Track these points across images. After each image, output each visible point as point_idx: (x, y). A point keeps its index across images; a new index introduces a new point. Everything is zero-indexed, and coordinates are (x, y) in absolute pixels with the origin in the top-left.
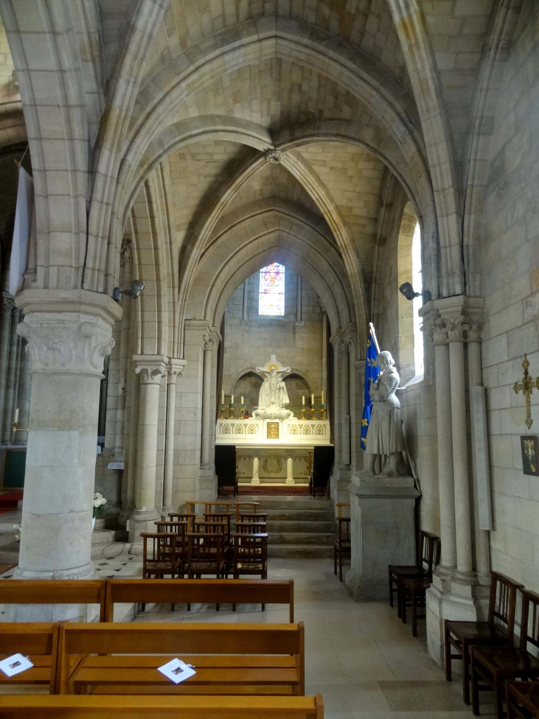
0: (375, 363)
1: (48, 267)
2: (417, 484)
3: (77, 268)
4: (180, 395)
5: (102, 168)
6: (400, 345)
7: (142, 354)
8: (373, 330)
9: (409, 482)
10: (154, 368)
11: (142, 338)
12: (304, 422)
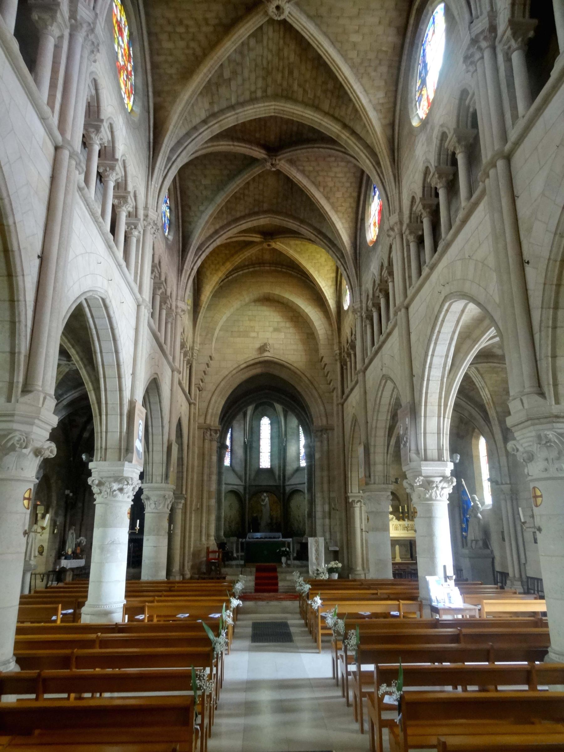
0: (466, 499)
1: (375, 476)
2: (492, 552)
3: (384, 476)
5: (391, 444)
6: (477, 490)
7: (351, 492)
8: (464, 483)
9: (488, 551)
10: (358, 499)
11: (351, 484)
12: (401, 522)
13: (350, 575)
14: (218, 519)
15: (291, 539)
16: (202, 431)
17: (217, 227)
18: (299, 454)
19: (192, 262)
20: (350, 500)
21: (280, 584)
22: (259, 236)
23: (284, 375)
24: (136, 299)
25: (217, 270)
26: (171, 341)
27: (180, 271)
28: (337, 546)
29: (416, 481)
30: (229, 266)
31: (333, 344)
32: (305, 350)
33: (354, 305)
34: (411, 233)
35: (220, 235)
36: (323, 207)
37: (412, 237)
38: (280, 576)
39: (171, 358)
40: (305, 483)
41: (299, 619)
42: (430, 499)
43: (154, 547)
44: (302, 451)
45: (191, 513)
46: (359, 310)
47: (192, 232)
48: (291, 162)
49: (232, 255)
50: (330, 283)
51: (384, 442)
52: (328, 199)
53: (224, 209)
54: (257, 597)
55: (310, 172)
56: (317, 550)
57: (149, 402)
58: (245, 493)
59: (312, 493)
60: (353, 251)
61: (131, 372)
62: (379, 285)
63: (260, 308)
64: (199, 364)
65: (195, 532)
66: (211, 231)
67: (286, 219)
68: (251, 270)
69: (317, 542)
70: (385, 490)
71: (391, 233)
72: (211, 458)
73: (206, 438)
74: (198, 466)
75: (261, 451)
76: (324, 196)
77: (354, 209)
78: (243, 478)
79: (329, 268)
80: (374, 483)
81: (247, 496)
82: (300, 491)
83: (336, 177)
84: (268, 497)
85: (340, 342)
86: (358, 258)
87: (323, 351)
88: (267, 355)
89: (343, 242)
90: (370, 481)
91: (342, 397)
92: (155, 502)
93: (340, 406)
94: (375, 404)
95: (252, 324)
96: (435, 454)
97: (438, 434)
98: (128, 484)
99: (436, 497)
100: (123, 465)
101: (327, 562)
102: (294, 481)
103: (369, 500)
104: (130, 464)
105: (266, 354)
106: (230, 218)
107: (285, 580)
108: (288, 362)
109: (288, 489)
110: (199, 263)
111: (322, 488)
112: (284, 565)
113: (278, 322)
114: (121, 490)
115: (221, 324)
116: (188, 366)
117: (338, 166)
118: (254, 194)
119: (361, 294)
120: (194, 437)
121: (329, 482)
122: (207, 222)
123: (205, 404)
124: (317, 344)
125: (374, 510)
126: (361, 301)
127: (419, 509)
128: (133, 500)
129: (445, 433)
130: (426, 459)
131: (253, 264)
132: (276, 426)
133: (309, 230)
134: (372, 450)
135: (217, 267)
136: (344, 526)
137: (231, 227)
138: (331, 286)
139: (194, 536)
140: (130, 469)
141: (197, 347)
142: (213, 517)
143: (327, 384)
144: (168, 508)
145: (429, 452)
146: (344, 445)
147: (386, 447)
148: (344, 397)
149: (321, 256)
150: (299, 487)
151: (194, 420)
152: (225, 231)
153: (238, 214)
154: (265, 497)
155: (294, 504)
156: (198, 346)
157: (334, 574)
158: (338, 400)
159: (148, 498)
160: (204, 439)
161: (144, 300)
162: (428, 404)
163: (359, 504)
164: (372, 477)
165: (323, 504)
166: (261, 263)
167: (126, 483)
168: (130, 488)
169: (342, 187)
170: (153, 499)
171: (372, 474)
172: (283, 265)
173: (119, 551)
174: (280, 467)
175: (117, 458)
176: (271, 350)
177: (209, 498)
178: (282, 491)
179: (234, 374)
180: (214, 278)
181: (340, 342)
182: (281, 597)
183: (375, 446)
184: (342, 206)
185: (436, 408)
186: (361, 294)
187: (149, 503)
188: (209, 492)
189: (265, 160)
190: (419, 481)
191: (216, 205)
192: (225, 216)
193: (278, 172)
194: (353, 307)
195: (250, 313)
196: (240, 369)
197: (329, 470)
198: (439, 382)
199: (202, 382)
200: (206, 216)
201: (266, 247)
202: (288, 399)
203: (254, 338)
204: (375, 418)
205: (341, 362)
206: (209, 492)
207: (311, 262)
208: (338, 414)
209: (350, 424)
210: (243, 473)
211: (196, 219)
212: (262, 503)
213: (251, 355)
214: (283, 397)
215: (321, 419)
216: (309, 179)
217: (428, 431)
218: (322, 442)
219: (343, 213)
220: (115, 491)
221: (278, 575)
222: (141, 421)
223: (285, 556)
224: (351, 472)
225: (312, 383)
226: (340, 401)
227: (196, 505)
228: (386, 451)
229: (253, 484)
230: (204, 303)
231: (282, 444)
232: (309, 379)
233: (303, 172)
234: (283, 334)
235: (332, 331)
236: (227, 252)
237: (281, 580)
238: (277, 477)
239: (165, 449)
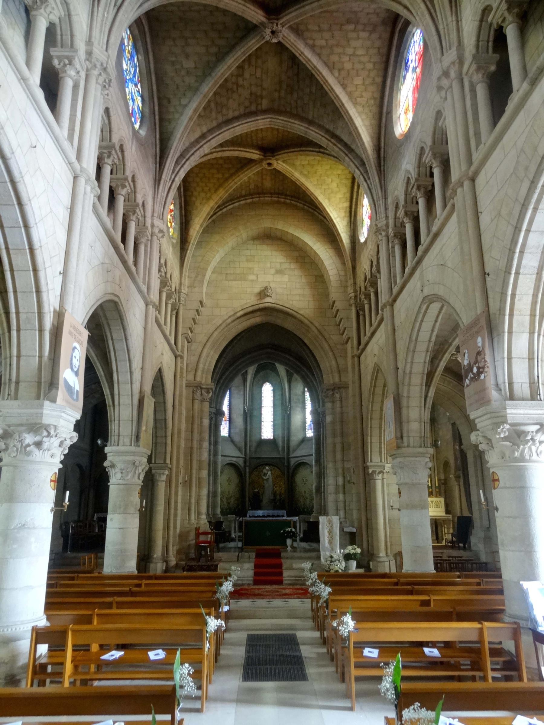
3: (421, 437)
4: (388, 485)
5: (429, 395)
7: (371, 461)
10: (380, 470)
11: (371, 452)
13: (371, 563)
14: (213, 494)
15: (297, 518)
17: (205, 130)
18: (304, 423)
19: (173, 172)
20: (371, 471)
21: (286, 574)
22: (258, 152)
23: (288, 325)
24: (73, 169)
25: (208, 199)
26: (145, 266)
27: (157, 181)
28: (353, 527)
29: (499, 430)
30: (222, 194)
31: (347, 287)
32: (314, 295)
33: (377, 222)
34: (478, 69)
35: (207, 139)
36: (337, 96)
37: (480, 76)
38: (286, 563)
39: (144, 288)
40: (312, 455)
41: (312, 629)
42: (522, 459)
43: (120, 529)
44: (309, 418)
45: (177, 486)
46: (385, 228)
47: (172, 133)
48: (296, 30)
49: (227, 180)
50: (343, 214)
51: (421, 392)
52: (344, 87)
53: (212, 105)
54: (257, 592)
55: (322, 47)
56: (330, 532)
57: (112, 339)
58: (245, 466)
59: (320, 465)
60: (375, 156)
61: (61, 268)
62: (417, 180)
63: (259, 247)
65: (183, 509)
66: (197, 134)
67: (290, 120)
68: (249, 201)
69: (330, 522)
70: (423, 455)
71: (445, 82)
72: (202, 422)
73: (196, 397)
74: (186, 431)
75: (262, 420)
76: (339, 82)
77: (378, 101)
79: (342, 196)
80: (408, 446)
81: (248, 470)
83: (354, 55)
84: (271, 470)
85: (355, 283)
86: (382, 164)
87: (335, 294)
88: (269, 301)
89: (363, 144)
90: (403, 443)
91: (358, 349)
92: (121, 469)
93: (356, 359)
94: (410, 341)
95: (250, 265)
96: (527, 392)
97: (529, 359)
98: (49, 435)
99: (530, 456)
100: (41, 406)
101: (343, 546)
102: (300, 452)
103: (402, 468)
104: (53, 405)
105: (267, 300)
106: (220, 119)
107: (292, 569)
108: (295, 309)
109: (293, 462)
110: (182, 174)
111: (335, 456)
112: (289, 548)
113: (281, 263)
114: (38, 444)
115: (214, 263)
116: (174, 312)
117: (358, 38)
118: (251, 85)
119: (386, 209)
120: (181, 396)
121: (343, 449)
122: (191, 119)
124: (327, 288)
125: (408, 480)
126: (387, 217)
127: (501, 474)
128: (61, 462)
129: (540, 357)
130: (512, 397)
131: (251, 195)
132: (279, 393)
133: (320, 133)
134: (404, 403)
135: (209, 195)
136: (363, 501)
137: (222, 130)
138: (345, 216)
139: (182, 514)
140: (55, 413)
141: (185, 290)
142: (204, 492)
143: (340, 334)
144: (139, 478)
145: (516, 387)
146: (362, 405)
147: (423, 399)
148: (361, 347)
149: (332, 181)
150: (306, 460)
151: (181, 376)
152: (215, 135)
153: (231, 115)
154: (267, 470)
155: (299, 478)
156: (187, 289)
157: (352, 561)
158: (352, 352)
159: (113, 466)
160: (193, 399)
161: (82, 169)
162: (515, 312)
163: (380, 475)
164: (405, 439)
165: (336, 477)
166: (259, 192)
167: (45, 433)
168: (55, 442)
169: (363, 69)
170: (119, 466)
171: (405, 435)
172: (286, 195)
173: (33, 540)
174: (283, 438)
175: (34, 395)
176: (273, 296)
177: (200, 469)
178: (286, 464)
179: (229, 324)
180: (204, 209)
181: (355, 283)
182: (287, 591)
183: (408, 397)
184: (362, 96)
185: (527, 319)
186: (386, 209)
187: (114, 472)
188: (200, 462)
189: (262, 24)
190: (504, 430)
191: (202, 96)
192: (214, 114)
193: (281, 47)
194: (376, 225)
195: (248, 252)
196: (236, 317)
197: (342, 436)
198: (534, 277)
199: (192, 332)
200: (189, 112)
201: (266, 166)
202: (291, 359)
203: (253, 281)
204: (409, 360)
205: (357, 307)
206: (200, 462)
207: (320, 188)
208: (353, 368)
209: (369, 377)
211: (177, 116)
213: (248, 301)
214: (287, 356)
215: (333, 376)
216: (320, 58)
217: (514, 355)
218: (333, 402)
219: (363, 106)
220: (28, 445)
221: (283, 561)
222: (76, 344)
223: (290, 537)
224: (371, 436)
226: (356, 352)
227: (184, 478)
228: (423, 405)
229: (254, 456)
230: (193, 238)
231: (286, 413)
233: (312, 47)
234: (287, 276)
235: (346, 271)
236: (220, 176)
237: (287, 569)
238: (280, 449)
239: (136, 402)
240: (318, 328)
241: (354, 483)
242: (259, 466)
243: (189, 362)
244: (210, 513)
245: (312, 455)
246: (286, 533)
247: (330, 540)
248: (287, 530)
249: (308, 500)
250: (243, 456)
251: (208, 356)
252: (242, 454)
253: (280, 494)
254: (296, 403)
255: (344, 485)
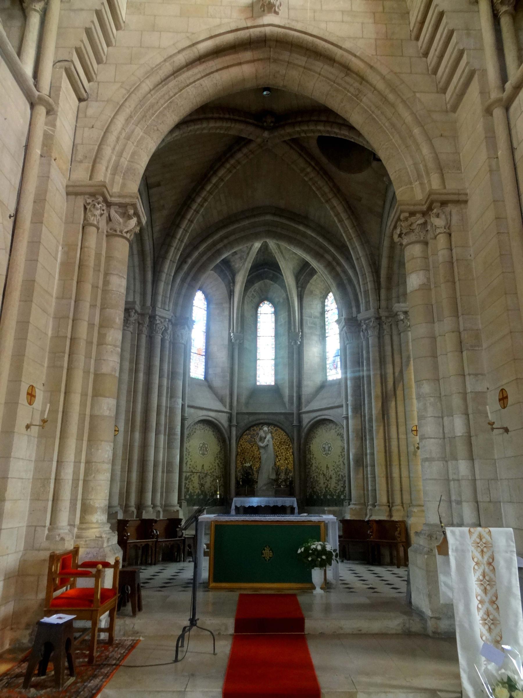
16: (80, 202)
18: (324, 358)
40: (342, 406)
58: (230, 426)
59: (362, 416)
64: (74, 10)
73: (93, 220)
75: (258, 357)
78: (228, 401)
81: (234, 432)
82: (330, 421)
84: (271, 433)
93: (498, 112)
105: (269, 19)
109: (306, 419)
112: (318, 591)
123: (97, 134)
132: (284, 315)
151: (46, 155)
174: (291, 383)
176: (283, 11)
177: (97, 394)
178: (295, 423)
197: (456, 314)
202: (309, 232)
210: (227, 392)
212: (261, 444)
214: (301, 228)
218: (426, 243)
225: (394, 90)
231: (296, 343)
232: (383, 78)
238: (286, 399)
240: (388, 77)
241: (507, 430)
242: (253, 426)
243: (78, 141)
244: (158, 503)
245: (342, 406)
246: (309, 555)
247: (488, 614)
248: (314, 546)
249: (334, 481)
250: (227, 410)
251: (128, 138)
252: (225, 406)
253: (287, 472)
254: (311, 328)
255: (469, 439)
